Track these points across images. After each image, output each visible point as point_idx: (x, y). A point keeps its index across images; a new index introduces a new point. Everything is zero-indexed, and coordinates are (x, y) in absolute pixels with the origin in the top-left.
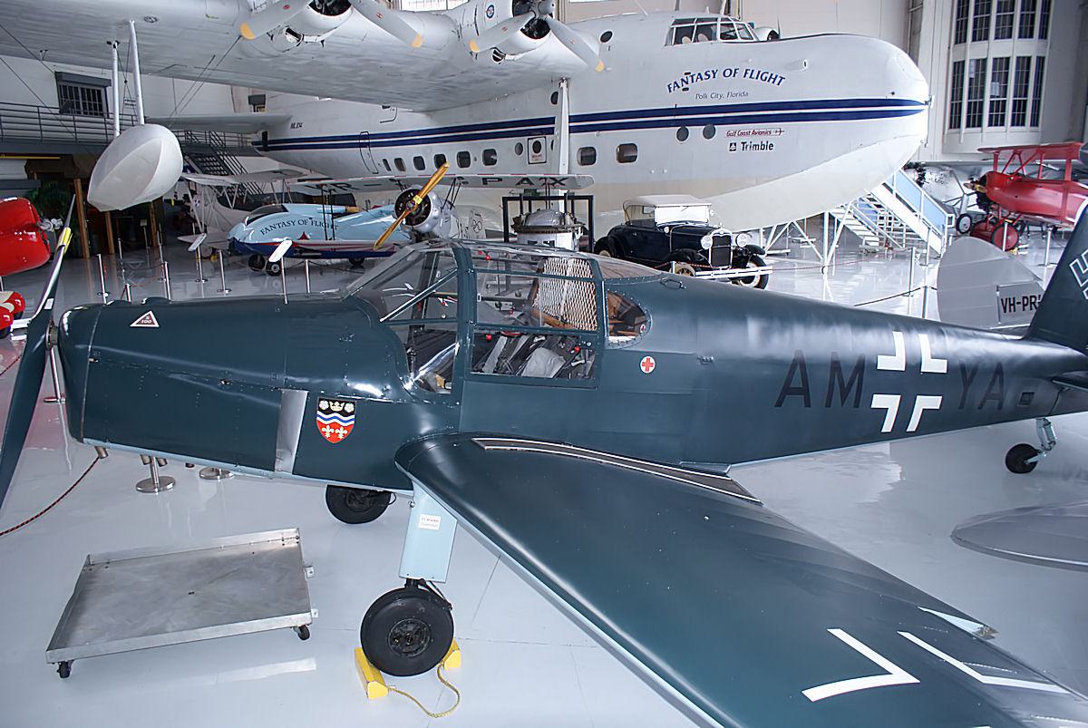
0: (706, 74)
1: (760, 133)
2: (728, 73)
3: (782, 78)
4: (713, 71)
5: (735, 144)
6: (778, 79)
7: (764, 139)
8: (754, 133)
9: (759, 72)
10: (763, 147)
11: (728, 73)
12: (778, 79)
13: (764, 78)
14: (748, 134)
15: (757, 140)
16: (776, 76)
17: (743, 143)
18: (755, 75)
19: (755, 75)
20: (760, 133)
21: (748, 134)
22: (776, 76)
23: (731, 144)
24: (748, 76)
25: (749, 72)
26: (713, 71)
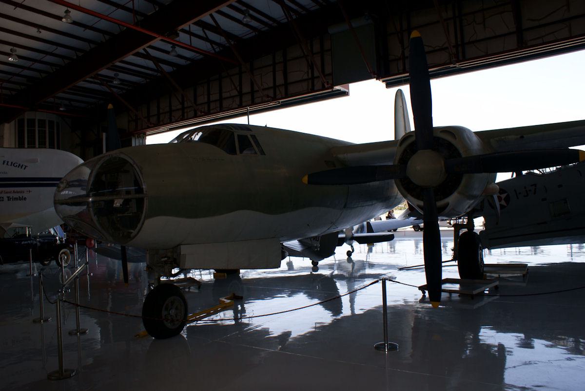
1: (18, 192)
3: (26, 166)
5: (3, 198)
6: (24, 167)
7: (20, 195)
8: (14, 192)
9: (12, 163)
10: (20, 199)
12: (24, 167)
14: (10, 192)
15: (16, 195)
16: (23, 165)
17: (8, 197)
18: (10, 163)
19: (10, 163)
20: (18, 192)
21: (10, 192)
22: (23, 165)
23: (3, 198)
24: (5, 164)
25: (6, 162)
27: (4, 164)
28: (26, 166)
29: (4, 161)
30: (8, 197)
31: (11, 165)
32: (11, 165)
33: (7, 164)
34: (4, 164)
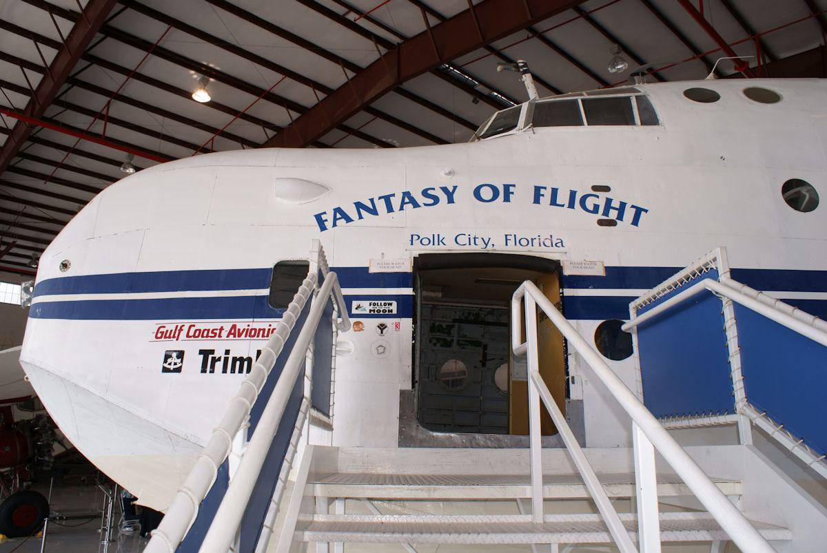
0: (425, 193)
2: (486, 193)
4: (445, 189)
5: (181, 355)
6: (629, 214)
11: (486, 193)
12: (629, 214)
13: (590, 203)
16: (623, 205)
17: (205, 353)
18: (563, 198)
19: (563, 198)
22: (623, 205)
23: (167, 357)
25: (547, 194)
26: (445, 189)
27: (537, 201)
28: (639, 211)
29: (537, 189)
30: (205, 353)
31: (571, 205)
32: (571, 205)
33: (553, 202)
34: (537, 201)
